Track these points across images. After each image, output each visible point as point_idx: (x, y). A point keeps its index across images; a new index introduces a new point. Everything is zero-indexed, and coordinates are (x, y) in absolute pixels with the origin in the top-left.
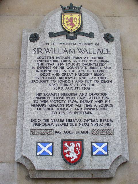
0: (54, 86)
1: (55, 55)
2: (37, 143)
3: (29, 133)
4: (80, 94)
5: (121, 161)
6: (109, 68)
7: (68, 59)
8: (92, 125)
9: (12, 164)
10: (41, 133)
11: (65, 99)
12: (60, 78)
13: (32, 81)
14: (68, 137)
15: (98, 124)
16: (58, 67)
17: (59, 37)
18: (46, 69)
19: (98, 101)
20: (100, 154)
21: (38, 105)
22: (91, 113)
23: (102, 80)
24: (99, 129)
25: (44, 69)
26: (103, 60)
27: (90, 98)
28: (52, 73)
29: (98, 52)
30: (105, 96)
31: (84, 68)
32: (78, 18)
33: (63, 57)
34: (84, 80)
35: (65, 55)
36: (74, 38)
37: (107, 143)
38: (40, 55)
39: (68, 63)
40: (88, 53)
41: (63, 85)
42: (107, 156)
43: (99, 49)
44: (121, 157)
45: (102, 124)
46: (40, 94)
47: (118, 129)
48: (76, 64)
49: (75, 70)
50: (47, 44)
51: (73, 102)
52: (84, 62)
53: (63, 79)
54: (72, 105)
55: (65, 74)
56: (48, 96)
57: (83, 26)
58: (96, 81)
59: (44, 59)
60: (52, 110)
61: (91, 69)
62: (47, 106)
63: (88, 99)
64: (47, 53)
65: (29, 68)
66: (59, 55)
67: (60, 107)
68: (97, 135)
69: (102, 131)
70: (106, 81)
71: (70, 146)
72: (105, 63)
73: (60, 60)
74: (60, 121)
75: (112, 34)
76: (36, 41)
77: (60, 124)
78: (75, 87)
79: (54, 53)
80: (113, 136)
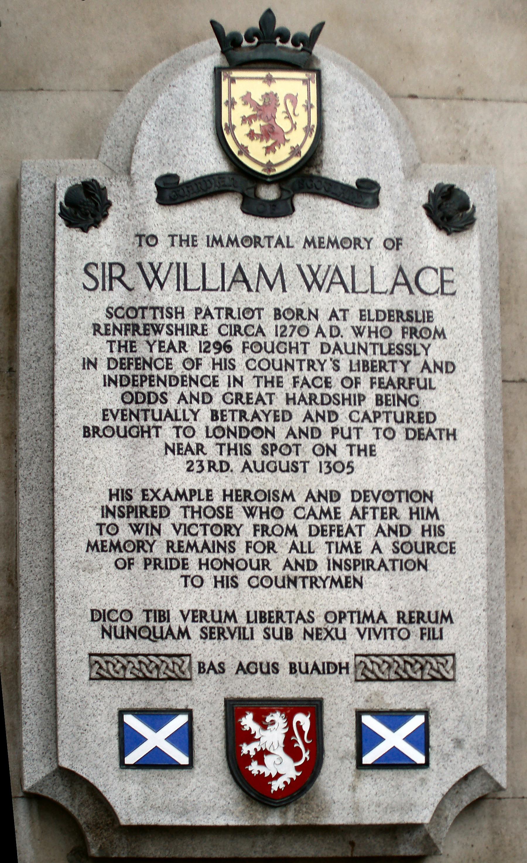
1: (189, 301)
7: (250, 322)
11: (239, 517)
12: (214, 416)
14: (256, 687)
16: (207, 359)
17: (205, 204)
18: (147, 372)
19: (390, 528)
20: (394, 762)
21: (116, 547)
23: (411, 425)
29: (396, 284)
30: (421, 505)
31: (329, 365)
34: (325, 427)
35: (238, 298)
36: (281, 209)
38: (118, 296)
39: (251, 340)
46: (127, 494)
52: (328, 335)
54: (270, 547)
56: (162, 503)
60: (183, 568)
62: (160, 551)
64: (150, 286)
66: (207, 300)
67: (216, 555)
68: (379, 679)
70: (430, 433)
72: (426, 343)
77: (221, 634)
78: (284, 460)
79: (186, 289)
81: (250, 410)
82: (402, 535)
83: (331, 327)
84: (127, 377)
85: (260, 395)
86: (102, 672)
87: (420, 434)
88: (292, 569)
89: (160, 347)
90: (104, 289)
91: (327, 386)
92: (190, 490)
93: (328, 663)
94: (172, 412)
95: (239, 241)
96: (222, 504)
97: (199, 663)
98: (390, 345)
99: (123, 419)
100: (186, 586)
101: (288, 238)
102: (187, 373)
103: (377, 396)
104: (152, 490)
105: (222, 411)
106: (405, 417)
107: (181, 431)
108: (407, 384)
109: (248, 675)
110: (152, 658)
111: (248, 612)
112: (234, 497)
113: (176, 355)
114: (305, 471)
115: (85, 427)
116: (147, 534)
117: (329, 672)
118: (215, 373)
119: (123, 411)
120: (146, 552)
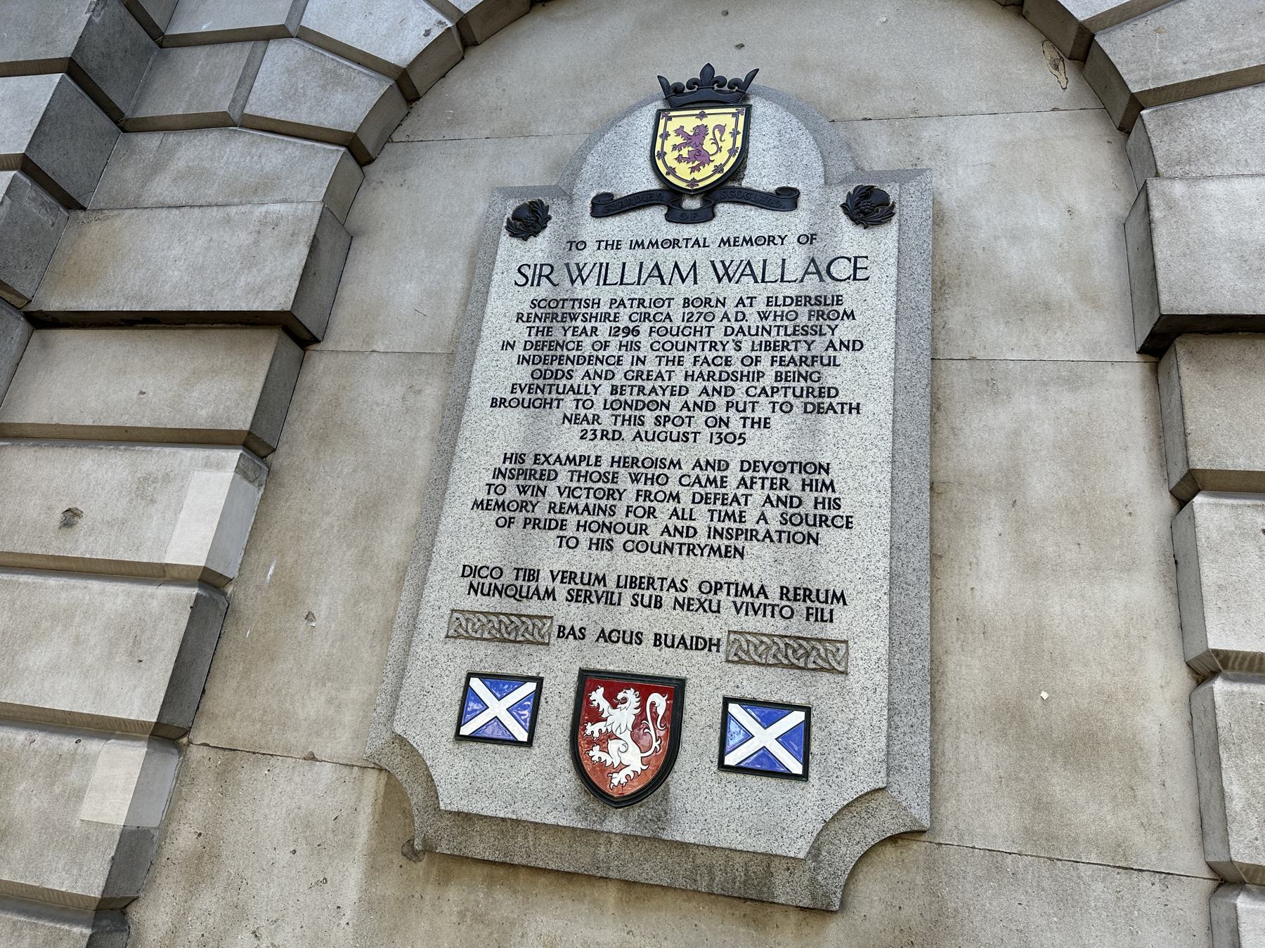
0: (585, 425)
2: (470, 675)
4: (698, 464)
6: (855, 345)
7: (660, 310)
10: (494, 632)
11: (624, 482)
12: (614, 390)
13: (495, 403)
15: (769, 609)
16: (614, 342)
17: (632, 215)
18: (559, 352)
19: (779, 499)
20: (764, 767)
21: (501, 506)
23: (811, 399)
25: (551, 353)
26: (826, 309)
27: (743, 482)
28: (586, 367)
29: (806, 273)
30: (816, 476)
31: (731, 346)
32: (729, 129)
33: (641, 302)
34: (720, 401)
35: (654, 290)
37: (808, 710)
38: (544, 291)
39: (658, 325)
40: (759, 280)
41: (624, 420)
42: (803, 785)
43: (813, 260)
45: (787, 612)
46: (520, 458)
47: (870, 644)
49: (688, 357)
50: (577, 245)
51: (660, 496)
52: (733, 320)
54: (650, 512)
55: (639, 375)
57: (752, 160)
58: (777, 407)
59: (559, 311)
61: (763, 354)
62: (541, 512)
63: (731, 489)
64: (573, 282)
66: (622, 293)
67: (595, 518)
70: (831, 407)
72: (833, 324)
73: (624, 313)
74: (586, 581)
75: (887, 190)
76: (536, 234)
77: (588, 597)
79: (605, 284)
80: (840, 678)
82: (791, 506)
86: (460, 630)
87: (819, 407)
93: (698, 638)
102: (595, 353)
108: (809, 362)
109: (610, 645)
110: (513, 618)
117: (697, 648)
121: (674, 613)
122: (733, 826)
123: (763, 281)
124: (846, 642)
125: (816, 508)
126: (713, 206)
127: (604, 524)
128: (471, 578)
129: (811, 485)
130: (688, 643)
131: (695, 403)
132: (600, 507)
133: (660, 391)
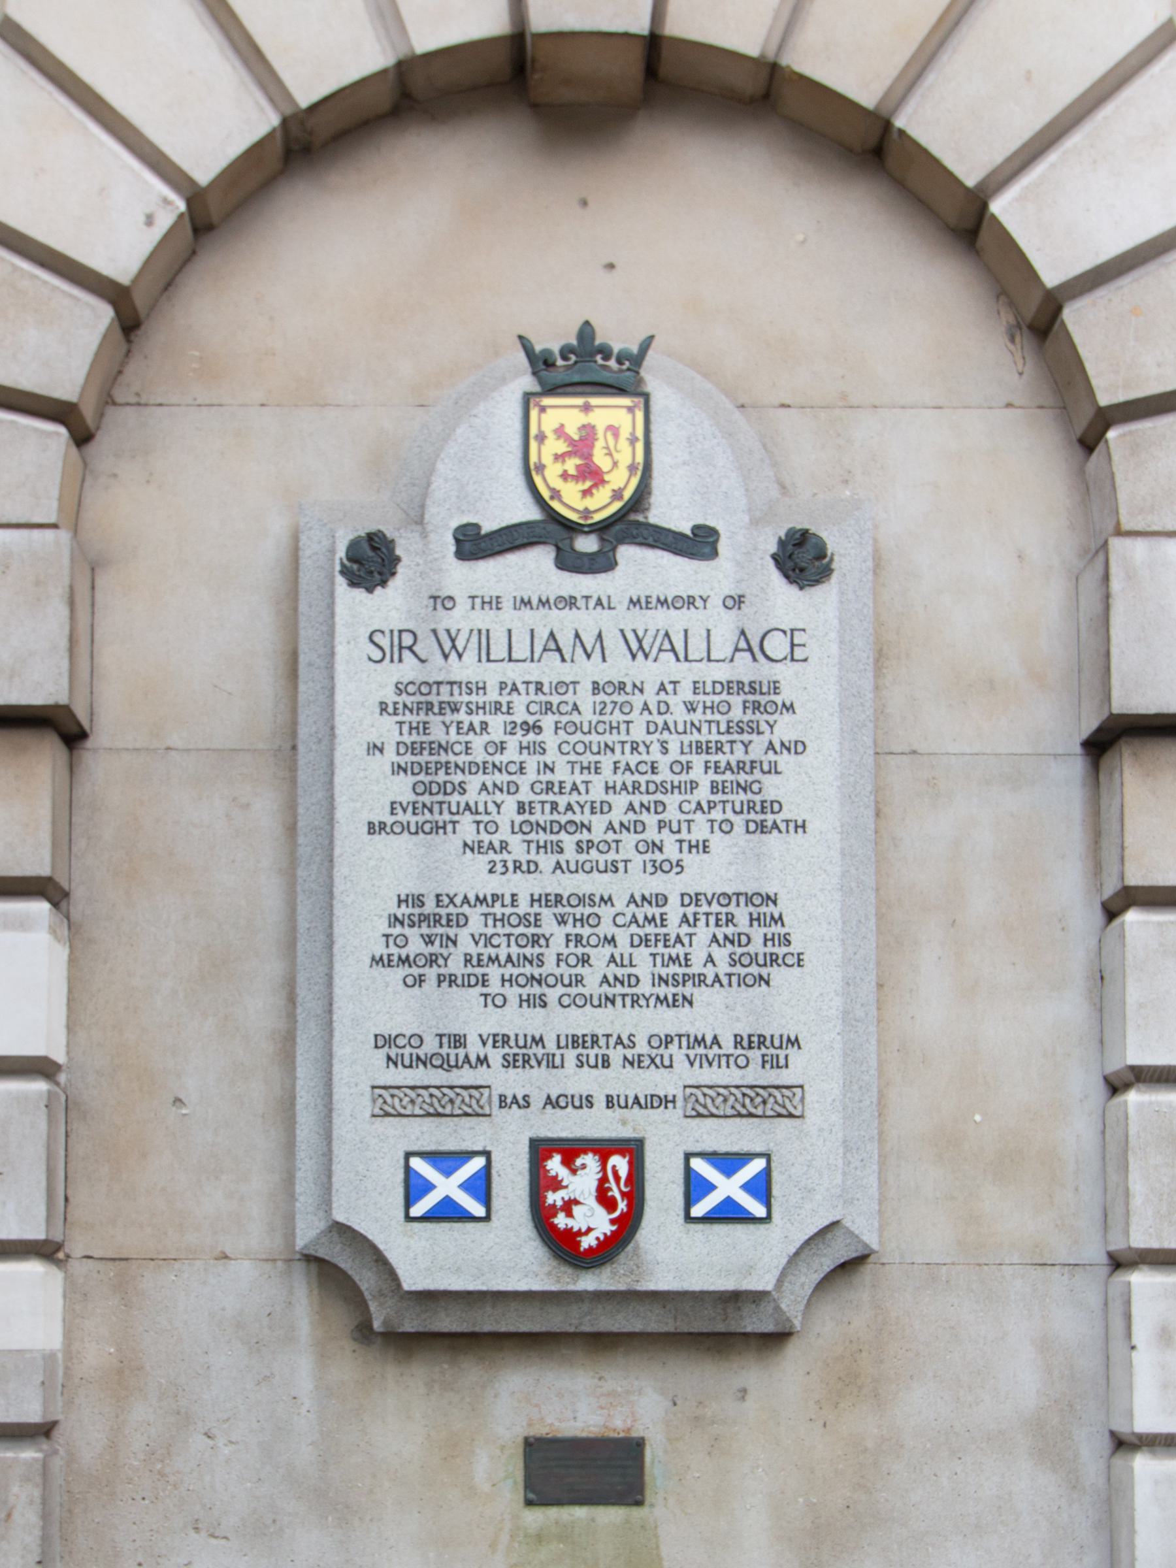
0: (492, 856)
1: (492, 675)
2: (408, 1155)
3: (366, 1107)
5: (837, 1252)
6: (796, 747)
7: (564, 698)
8: (692, 1064)
9: (279, 1263)
10: (426, 1106)
11: (549, 925)
12: (521, 808)
13: (372, 828)
15: (724, 1060)
16: (512, 743)
17: (512, 558)
18: (443, 758)
20: (729, 1214)
21: (405, 961)
22: (686, 1004)
23: (752, 816)
24: (725, 1087)
26: (763, 700)
27: (685, 919)
28: (480, 778)
29: (737, 650)
30: (763, 909)
31: (655, 748)
32: (625, 433)
34: (650, 820)
35: (550, 670)
36: (602, 563)
37: (768, 1156)
38: (409, 669)
39: (565, 719)
40: (682, 656)
41: (538, 847)
42: (767, 1226)
43: (743, 633)
44: (838, 1232)
45: (742, 1061)
46: (419, 900)
48: (611, 728)
49: (607, 761)
52: (655, 711)
53: (538, 817)
54: (585, 960)
55: (549, 786)
56: (460, 910)
59: (433, 698)
60: (483, 985)
62: (456, 966)
63: (673, 927)
64: (446, 657)
65: (349, 748)
66: (513, 673)
67: (521, 970)
68: (713, 1115)
69: (744, 1095)
70: (775, 826)
71: (574, 1172)
72: (771, 719)
73: (519, 702)
74: (521, 1043)
75: (824, 535)
76: (383, 583)
77: (526, 1061)
78: (602, 859)
79: (488, 660)
80: (797, 1122)
81: (562, 801)
82: (740, 945)
83: (659, 702)
84: (419, 764)
85: (574, 784)
86: (386, 1108)
87: (763, 826)
88: (610, 985)
89: (458, 728)
90: (392, 661)
91: (653, 773)
92: (493, 895)
93: (652, 1096)
94: (472, 805)
95: (552, 601)
96: (529, 910)
97: (500, 1096)
98: (728, 722)
99: (414, 813)
100: (486, 1006)
101: (609, 597)
103: (712, 782)
104: (448, 895)
105: (530, 803)
106: (745, 807)
107: (482, 826)
108: (747, 768)
109: (558, 1110)
110: (445, 1090)
111: (558, 1036)
112: (543, 903)
113: (477, 737)
114: (626, 871)
115: (369, 823)
116: (441, 946)
117: (652, 1107)
118: (522, 758)
119: (414, 803)
120: (439, 966)
121: (625, 1071)
122: (703, 1270)
123: (686, 659)
124: (801, 1087)
125: (765, 945)
126: (614, 549)
127: (533, 977)
128: (386, 1048)
129: (758, 919)
130: (642, 1101)
131: (622, 824)
132: (525, 958)
133: (577, 808)
